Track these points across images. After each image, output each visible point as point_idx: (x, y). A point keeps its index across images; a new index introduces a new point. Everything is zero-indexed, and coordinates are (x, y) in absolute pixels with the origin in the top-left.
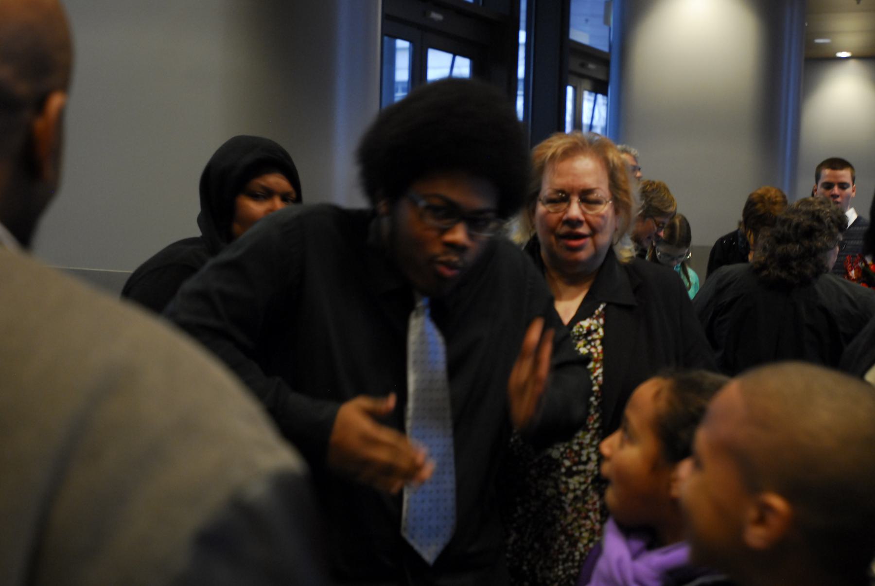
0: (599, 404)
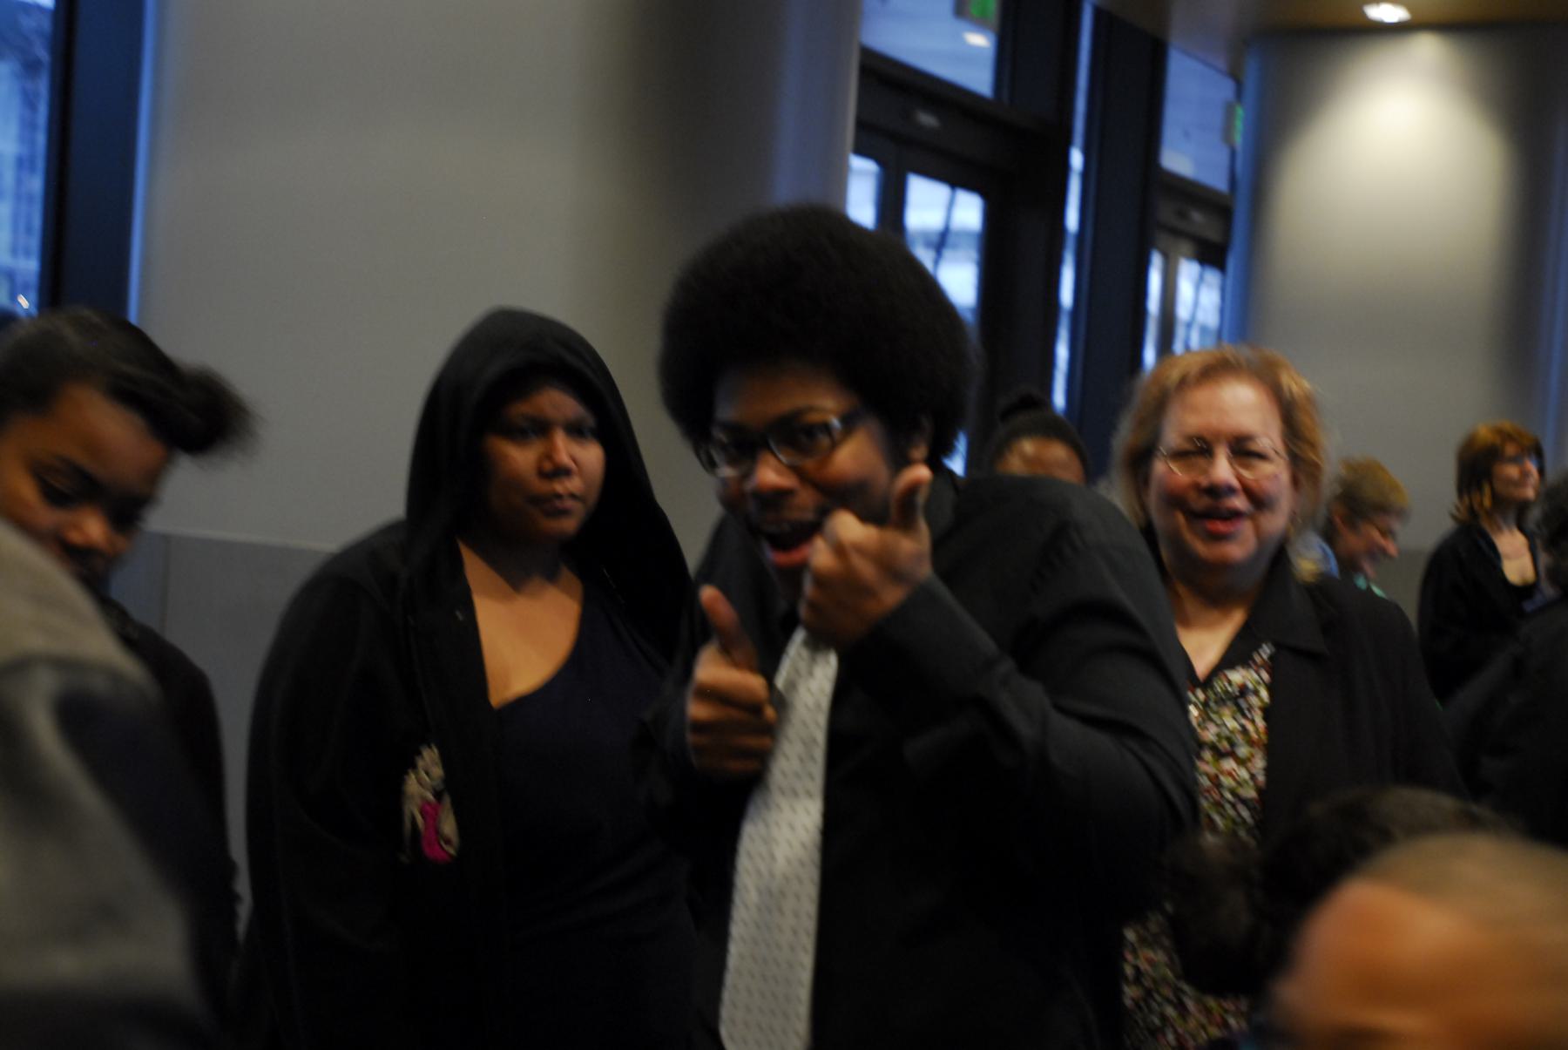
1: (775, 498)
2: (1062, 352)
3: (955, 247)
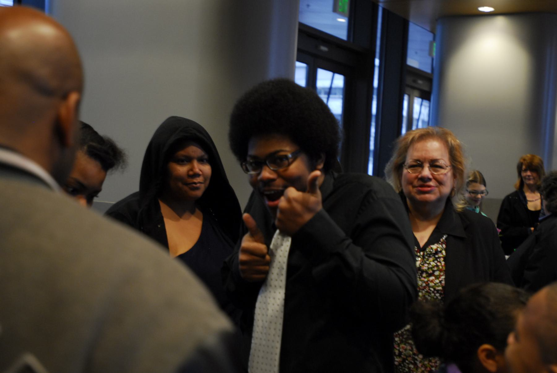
0: (441, 299)
1: (269, 181)
2: (373, 130)
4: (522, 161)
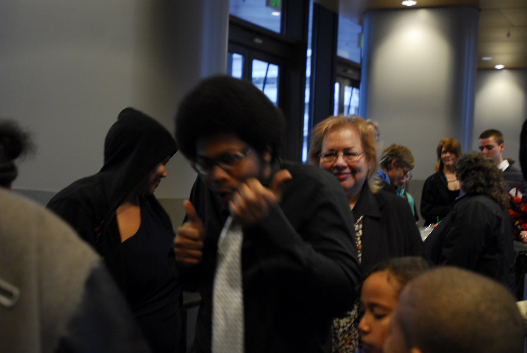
2: (306, 118)
3: (269, 83)
4: (441, 144)
